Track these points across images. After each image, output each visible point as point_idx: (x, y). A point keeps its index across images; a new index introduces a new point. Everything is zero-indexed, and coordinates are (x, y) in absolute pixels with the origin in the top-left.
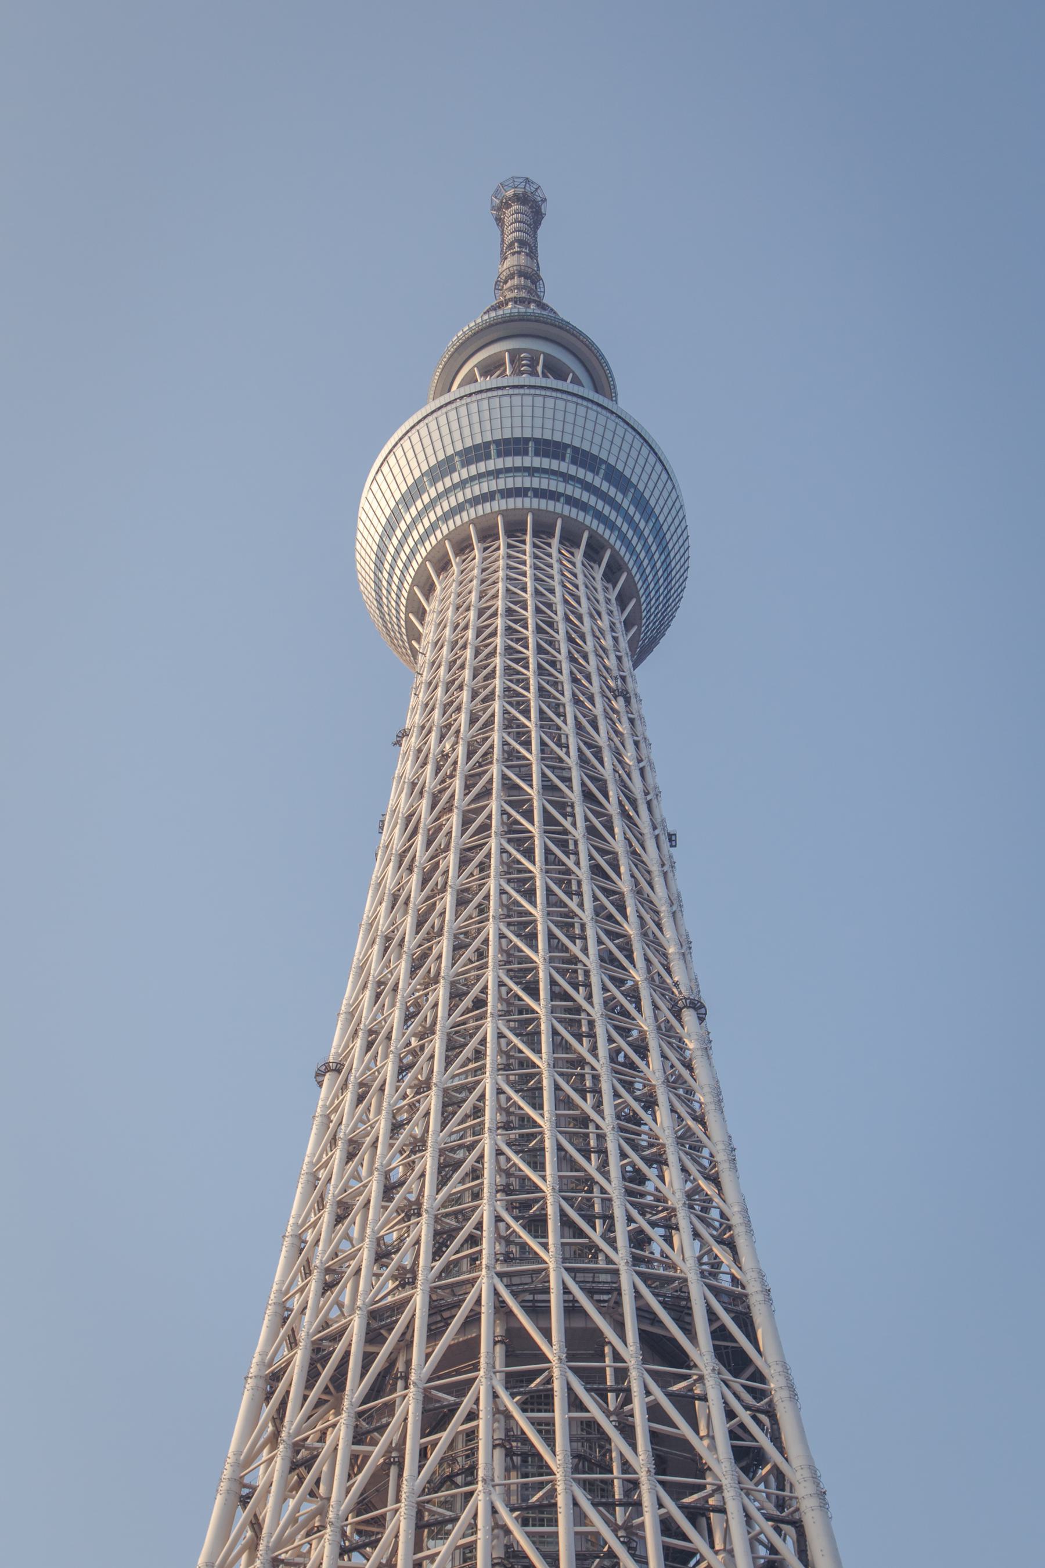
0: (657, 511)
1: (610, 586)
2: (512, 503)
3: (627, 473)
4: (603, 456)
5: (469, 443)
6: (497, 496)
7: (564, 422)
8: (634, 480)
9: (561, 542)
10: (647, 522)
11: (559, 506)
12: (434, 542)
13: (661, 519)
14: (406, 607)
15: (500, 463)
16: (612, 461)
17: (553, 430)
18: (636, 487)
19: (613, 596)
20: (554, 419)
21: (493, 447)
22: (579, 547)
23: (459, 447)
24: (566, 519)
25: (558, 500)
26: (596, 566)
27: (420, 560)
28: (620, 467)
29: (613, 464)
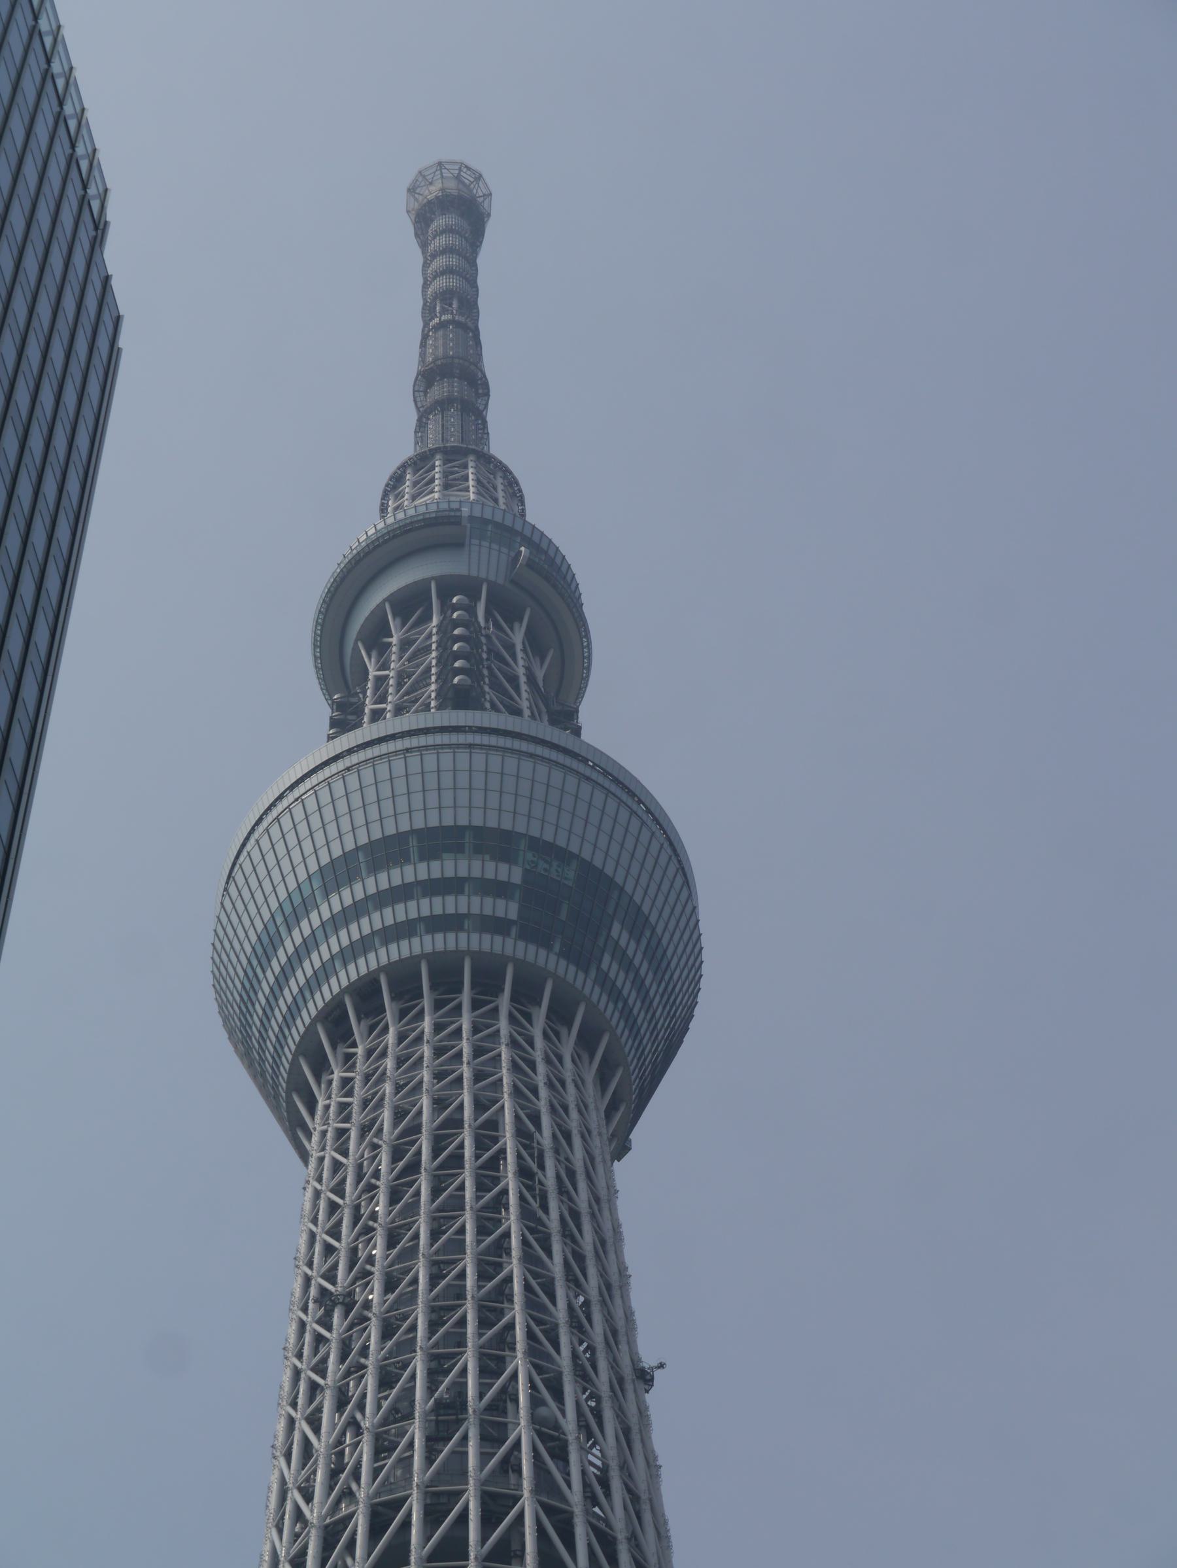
0: (653, 919)
1: (585, 1057)
2: (439, 942)
3: (609, 871)
4: (574, 848)
5: (377, 835)
6: (421, 927)
7: (516, 795)
8: (619, 879)
9: (514, 999)
10: (638, 942)
11: (510, 942)
12: (328, 997)
13: (659, 930)
14: (287, 1083)
15: (422, 871)
16: (586, 855)
17: (500, 810)
18: (622, 889)
19: (590, 1075)
20: (502, 774)
21: (413, 842)
22: (539, 1004)
23: (363, 840)
24: (520, 965)
25: (508, 934)
26: (564, 1031)
27: (307, 1021)
28: (598, 862)
29: (588, 858)
